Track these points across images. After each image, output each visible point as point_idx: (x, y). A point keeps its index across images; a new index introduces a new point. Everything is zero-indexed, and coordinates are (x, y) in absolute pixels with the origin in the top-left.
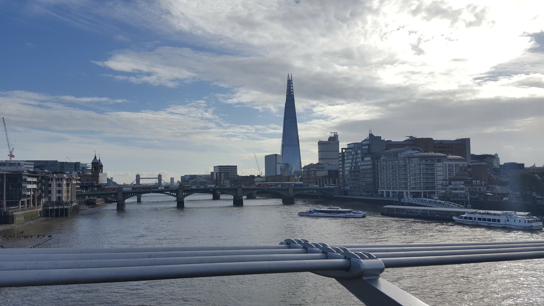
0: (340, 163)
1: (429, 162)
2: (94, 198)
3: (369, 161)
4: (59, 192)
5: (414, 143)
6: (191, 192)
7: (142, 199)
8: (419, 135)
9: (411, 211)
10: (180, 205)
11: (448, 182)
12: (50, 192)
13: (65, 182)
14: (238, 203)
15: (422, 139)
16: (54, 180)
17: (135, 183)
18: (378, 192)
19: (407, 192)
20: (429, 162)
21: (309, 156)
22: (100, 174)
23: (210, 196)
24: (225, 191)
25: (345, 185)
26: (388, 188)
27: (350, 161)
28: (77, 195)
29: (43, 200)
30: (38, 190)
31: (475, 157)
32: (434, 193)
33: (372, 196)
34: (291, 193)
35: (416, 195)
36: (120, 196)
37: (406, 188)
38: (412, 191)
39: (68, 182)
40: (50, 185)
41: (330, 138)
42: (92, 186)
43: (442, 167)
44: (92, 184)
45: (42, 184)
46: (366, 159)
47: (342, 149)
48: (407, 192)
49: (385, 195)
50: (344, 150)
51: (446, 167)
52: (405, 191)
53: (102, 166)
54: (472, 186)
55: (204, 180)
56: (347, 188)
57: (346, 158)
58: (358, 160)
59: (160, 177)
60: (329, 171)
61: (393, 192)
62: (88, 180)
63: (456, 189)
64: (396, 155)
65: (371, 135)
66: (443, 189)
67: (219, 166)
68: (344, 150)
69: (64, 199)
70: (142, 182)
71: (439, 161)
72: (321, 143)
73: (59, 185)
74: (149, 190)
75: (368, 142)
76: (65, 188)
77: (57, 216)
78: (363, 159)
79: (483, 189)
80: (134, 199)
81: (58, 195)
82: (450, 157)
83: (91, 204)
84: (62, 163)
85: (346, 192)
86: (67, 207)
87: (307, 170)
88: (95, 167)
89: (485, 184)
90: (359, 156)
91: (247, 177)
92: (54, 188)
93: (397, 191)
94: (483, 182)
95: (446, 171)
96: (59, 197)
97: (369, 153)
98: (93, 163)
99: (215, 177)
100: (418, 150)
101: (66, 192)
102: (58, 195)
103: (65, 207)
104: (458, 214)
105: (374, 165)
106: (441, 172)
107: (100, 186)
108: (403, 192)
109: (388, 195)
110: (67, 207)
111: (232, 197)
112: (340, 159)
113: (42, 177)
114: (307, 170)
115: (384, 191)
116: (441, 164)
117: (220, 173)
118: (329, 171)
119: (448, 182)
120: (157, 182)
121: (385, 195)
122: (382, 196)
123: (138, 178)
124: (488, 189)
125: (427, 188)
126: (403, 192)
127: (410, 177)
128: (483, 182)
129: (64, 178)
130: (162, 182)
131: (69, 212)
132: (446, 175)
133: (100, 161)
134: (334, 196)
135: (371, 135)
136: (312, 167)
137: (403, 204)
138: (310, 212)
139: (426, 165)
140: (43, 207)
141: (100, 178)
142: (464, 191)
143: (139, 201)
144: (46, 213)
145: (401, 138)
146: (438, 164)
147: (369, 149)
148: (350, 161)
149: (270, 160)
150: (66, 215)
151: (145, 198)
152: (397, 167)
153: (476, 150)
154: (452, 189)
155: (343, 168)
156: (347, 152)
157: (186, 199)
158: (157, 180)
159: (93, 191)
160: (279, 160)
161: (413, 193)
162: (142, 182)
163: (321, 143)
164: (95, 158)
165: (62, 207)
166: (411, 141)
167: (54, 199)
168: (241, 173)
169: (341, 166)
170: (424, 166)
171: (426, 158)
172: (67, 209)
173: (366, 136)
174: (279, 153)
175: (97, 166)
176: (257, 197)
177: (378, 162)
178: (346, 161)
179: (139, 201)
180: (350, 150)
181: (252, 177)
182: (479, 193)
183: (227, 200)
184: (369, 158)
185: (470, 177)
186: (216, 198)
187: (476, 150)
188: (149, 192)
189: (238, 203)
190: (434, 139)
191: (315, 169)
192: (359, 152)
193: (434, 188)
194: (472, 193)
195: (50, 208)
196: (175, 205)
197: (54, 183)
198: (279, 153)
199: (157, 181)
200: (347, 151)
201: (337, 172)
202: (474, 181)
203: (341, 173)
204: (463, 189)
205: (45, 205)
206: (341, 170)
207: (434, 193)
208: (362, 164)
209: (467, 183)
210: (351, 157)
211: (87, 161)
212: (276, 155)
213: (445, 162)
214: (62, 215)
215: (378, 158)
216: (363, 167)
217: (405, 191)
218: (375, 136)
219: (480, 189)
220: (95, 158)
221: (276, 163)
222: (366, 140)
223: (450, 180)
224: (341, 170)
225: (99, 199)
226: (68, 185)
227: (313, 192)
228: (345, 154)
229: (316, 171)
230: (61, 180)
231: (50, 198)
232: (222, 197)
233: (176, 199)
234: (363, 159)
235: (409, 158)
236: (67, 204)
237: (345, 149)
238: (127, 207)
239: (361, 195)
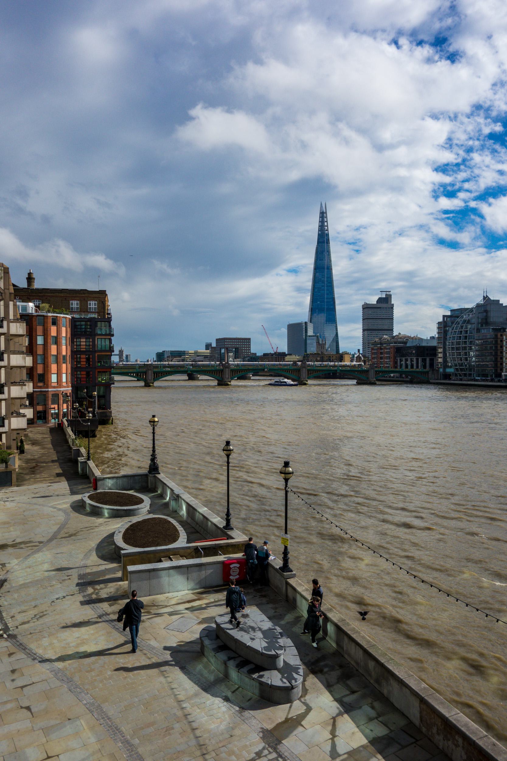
41: (380, 300)
47: (444, 316)
56: (448, 370)
65: (486, 298)
85: (447, 376)
97: (485, 322)
134: (431, 381)
135: (486, 298)
160: (310, 332)
173: (479, 300)
176: (310, 382)
177: (502, 335)
212: (306, 323)
218: (492, 299)
222: (478, 306)
227: (390, 377)
234: (478, 330)
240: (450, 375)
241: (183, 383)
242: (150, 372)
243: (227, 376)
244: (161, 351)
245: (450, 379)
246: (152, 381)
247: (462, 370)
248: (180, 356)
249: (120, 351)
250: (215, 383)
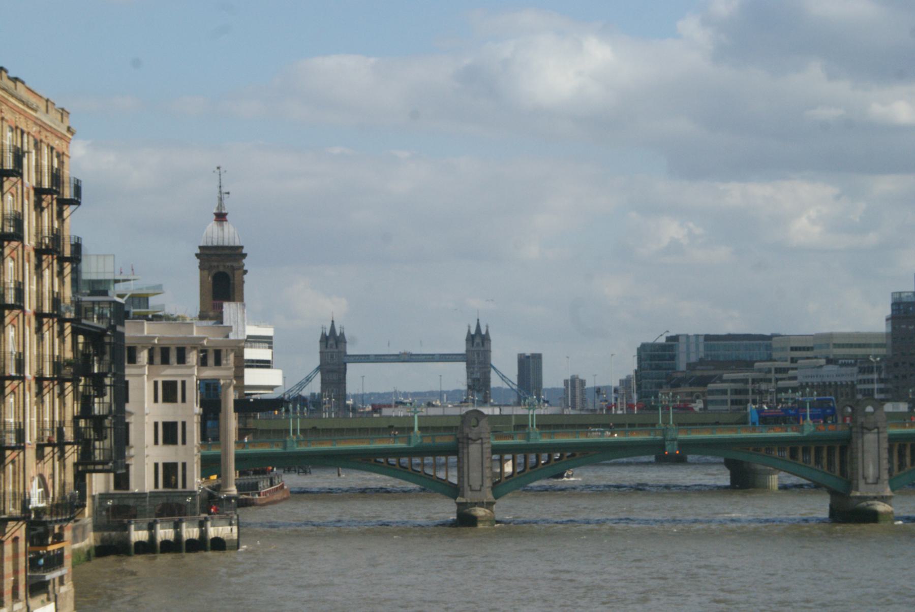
16: (143, 356)
17: (315, 387)
39: (209, 373)
55: (831, 374)
59: (478, 342)
70: (360, 381)
92: (146, 411)
96: (170, 469)
130: (495, 382)
167: (144, 480)
199: (455, 377)
230: (182, 359)
231: (122, 481)
241: (699, 508)
242: (474, 450)
243: (871, 471)
244: (663, 340)
246: (489, 496)
249: (471, 339)
250: (819, 506)
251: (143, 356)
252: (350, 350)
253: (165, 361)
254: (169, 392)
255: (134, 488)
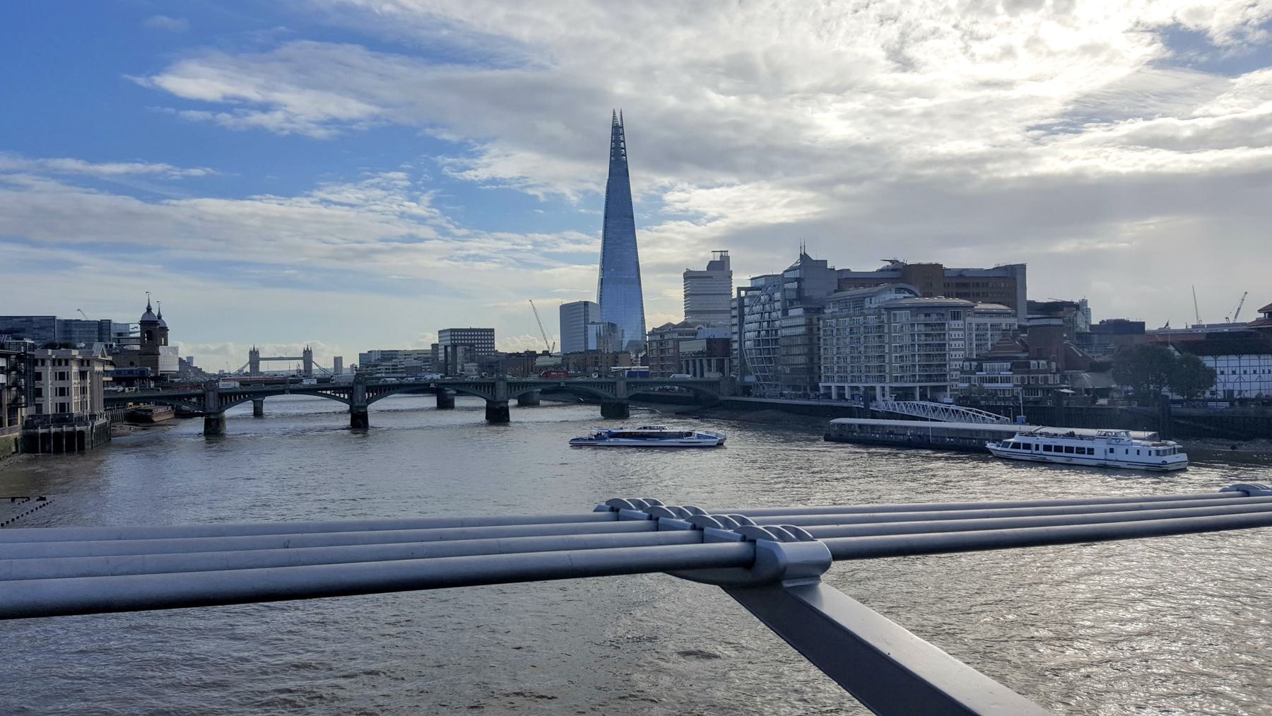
0: (735, 321)
1: (934, 319)
2: (147, 407)
3: (799, 316)
4: (62, 392)
5: (901, 275)
6: (383, 390)
7: (266, 409)
8: (911, 258)
9: (892, 431)
10: (359, 422)
11: (974, 364)
12: (39, 393)
13: (75, 369)
14: (497, 416)
15: (919, 265)
16: (49, 363)
17: (248, 369)
18: (817, 388)
19: (883, 388)
20: (934, 319)
21: (664, 305)
22: (161, 349)
23: (431, 401)
24: (465, 389)
25: (745, 372)
26: (843, 379)
27: (757, 317)
28: (105, 400)
29: (23, 413)
30: (9, 388)
31: (1036, 308)
32: (944, 388)
33: (806, 396)
34: (622, 392)
35: (904, 394)
36: (212, 403)
37: (881, 378)
38: (894, 385)
39: (83, 369)
40: (38, 376)
41: (712, 265)
42: (143, 377)
43: (963, 330)
44: (143, 372)
45: (19, 372)
46: (792, 312)
47: (739, 289)
48: (883, 388)
49: (834, 396)
50: (743, 293)
51: (971, 329)
52: (878, 386)
53: (165, 329)
54: (1029, 372)
55: (415, 363)
56: (750, 379)
57: (747, 310)
58: (774, 314)
59: (307, 355)
60: (709, 341)
61: (852, 388)
62: (132, 364)
63: (993, 380)
64: (859, 302)
65: (804, 257)
66: (963, 380)
67: (452, 330)
68: (743, 293)
69: (75, 410)
70: (264, 367)
71: (956, 316)
72: (690, 277)
73: (62, 376)
74: (281, 387)
75: (797, 274)
76: (75, 382)
77: (58, 451)
78: (785, 312)
79: (1053, 380)
80: (246, 409)
81: (61, 399)
82: (981, 306)
83: (141, 419)
84: (67, 323)
85: (747, 390)
86: (83, 428)
87: (658, 338)
88: (149, 333)
89: (1058, 369)
90: (778, 305)
91: (518, 355)
92: (49, 383)
93: (860, 385)
94: (1054, 365)
95: (971, 339)
96: (62, 406)
97: (800, 298)
98: (143, 323)
99: (442, 356)
100: (910, 292)
101: (79, 392)
102: (61, 399)
103: (78, 428)
104: (997, 437)
105: (809, 325)
106: (959, 342)
107: (160, 379)
108: (873, 388)
109: (841, 396)
110: (83, 428)
111: (483, 403)
112: (735, 313)
113: (19, 357)
114: (658, 338)
115: (833, 385)
116: (961, 322)
117: (454, 346)
118: (709, 341)
119: (974, 364)
120: (302, 368)
121: (834, 396)
122: (828, 396)
123: (254, 357)
124: (1064, 378)
125: (929, 378)
126: (873, 388)
127: (890, 353)
128: (1054, 365)
129: (73, 358)
130: (314, 367)
131: (87, 440)
132: (971, 349)
133: (159, 317)
134: (721, 398)
135: (804, 257)
136: (670, 332)
137: (874, 415)
138: (599, 437)
139: (926, 325)
140: (24, 428)
141: (161, 359)
142: (1010, 385)
143: (258, 413)
144: (30, 444)
145: (872, 266)
146: (953, 322)
147: (799, 290)
148: (757, 317)
149: (573, 315)
150: (82, 448)
151: (272, 405)
152: (862, 329)
153: (1038, 290)
154: (983, 380)
155: (741, 333)
156: (751, 297)
157: (372, 407)
158: (301, 362)
159: (149, 390)
160: (594, 316)
161: (896, 388)
162: (264, 367)
163: (689, 276)
164: (149, 309)
165: (70, 429)
166: (893, 270)
167: (50, 409)
168: (504, 344)
169: (735, 329)
170: (922, 328)
171: (927, 310)
172: (82, 433)
173: (793, 260)
174: (594, 299)
175: (153, 329)
177: (819, 319)
178: (747, 318)
179: (258, 413)
180: (757, 293)
181: (531, 355)
182: (1043, 389)
183: (471, 410)
184: (799, 311)
185: (1024, 351)
186: (445, 404)
187: (1038, 290)
188: (282, 392)
189: (497, 416)
190: (946, 266)
191: (676, 336)
192: (778, 295)
193: (943, 377)
194: (1028, 389)
195: (40, 431)
196: (346, 421)
197: (48, 372)
198: (594, 299)
200: (750, 293)
201: (727, 342)
202: (1033, 362)
203: (736, 346)
204: (1007, 380)
205: (28, 425)
206: (736, 337)
207: (944, 388)
208: (785, 323)
209: (1018, 366)
210: (758, 308)
211: (129, 317)
212: (586, 303)
213: (969, 320)
214: (70, 450)
215: (820, 310)
216: (785, 332)
217: (878, 386)
219: (1046, 379)
220: (149, 309)
221: (586, 322)
222: (792, 269)
223: (981, 359)
224: (736, 337)
225: (161, 409)
226: (83, 375)
228: (746, 301)
229: (679, 340)
230: (67, 364)
231: (39, 407)
232: (459, 402)
233: (346, 407)
234: (785, 312)
235: (888, 309)
236: (81, 420)
237: (746, 289)
238: (229, 428)
239: (782, 395)
240: (750, 387)
245: (749, 395)
247: (765, 378)
248: (391, 359)
251: (49, 363)
252: (261, 356)
253: (60, 364)
254: (62, 376)
255: (44, 412)
